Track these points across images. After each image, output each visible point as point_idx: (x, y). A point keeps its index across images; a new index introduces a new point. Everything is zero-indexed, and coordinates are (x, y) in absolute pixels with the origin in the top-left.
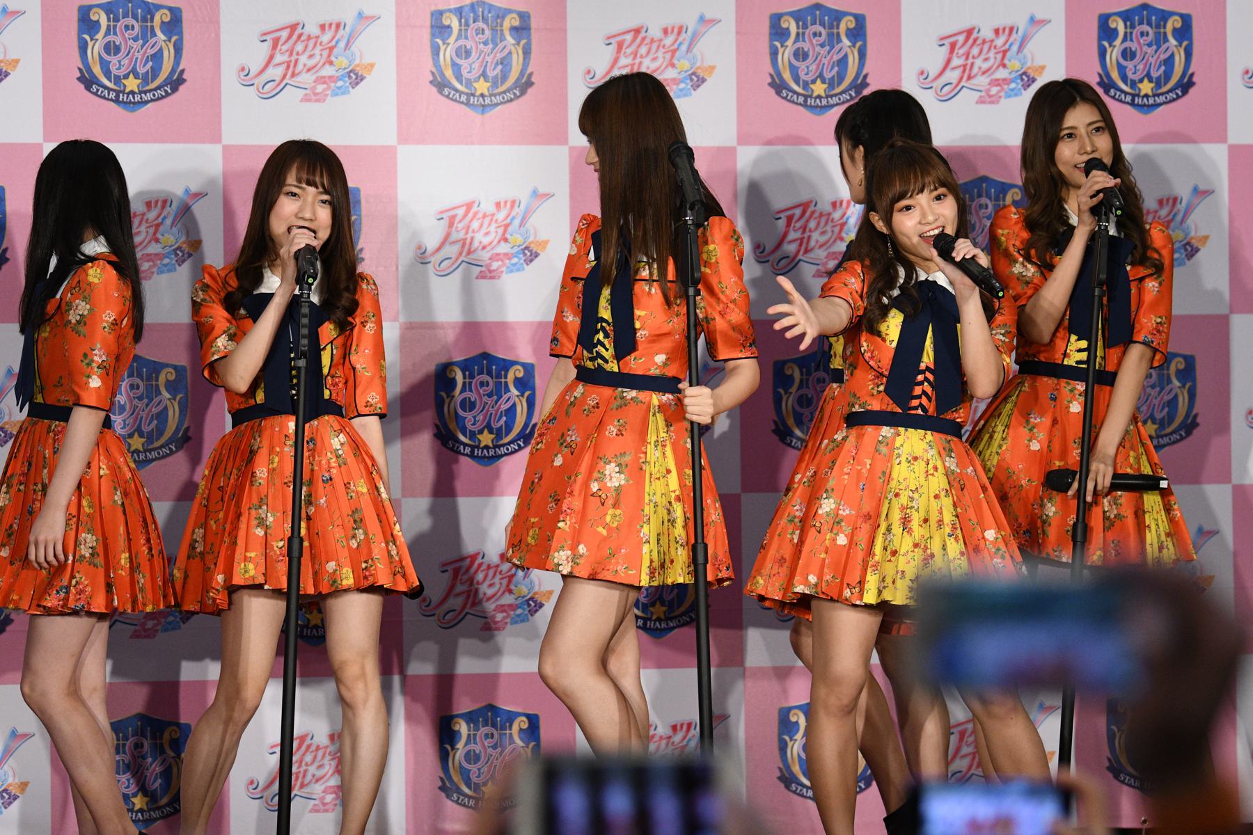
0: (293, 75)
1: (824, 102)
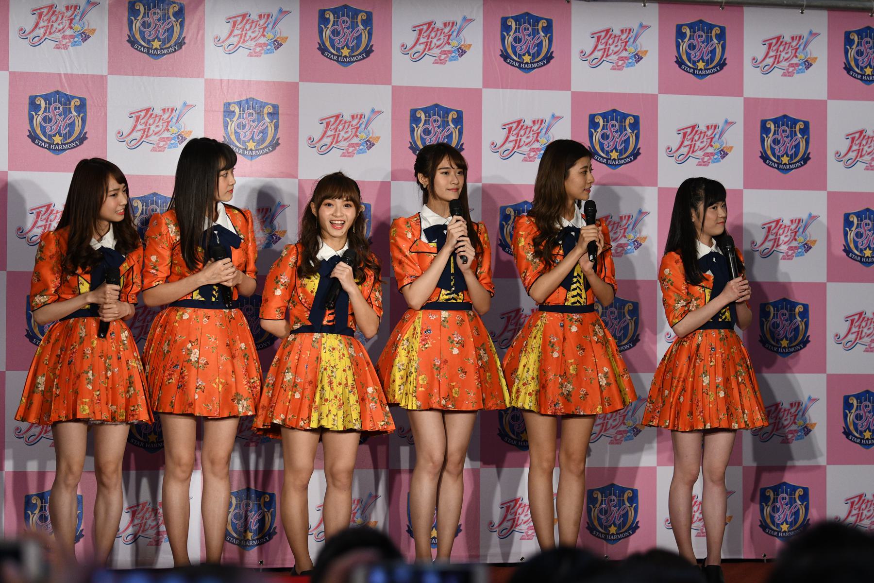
0: (147, 136)
1: (617, 162)
